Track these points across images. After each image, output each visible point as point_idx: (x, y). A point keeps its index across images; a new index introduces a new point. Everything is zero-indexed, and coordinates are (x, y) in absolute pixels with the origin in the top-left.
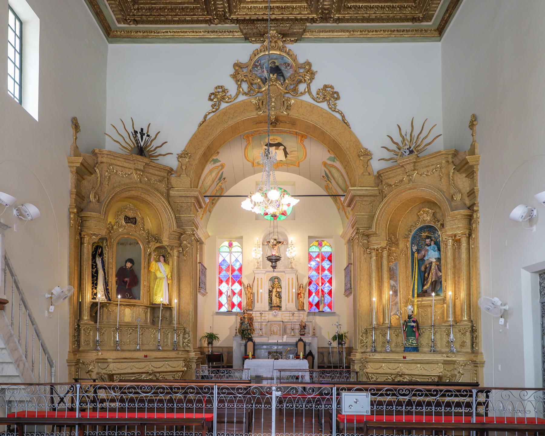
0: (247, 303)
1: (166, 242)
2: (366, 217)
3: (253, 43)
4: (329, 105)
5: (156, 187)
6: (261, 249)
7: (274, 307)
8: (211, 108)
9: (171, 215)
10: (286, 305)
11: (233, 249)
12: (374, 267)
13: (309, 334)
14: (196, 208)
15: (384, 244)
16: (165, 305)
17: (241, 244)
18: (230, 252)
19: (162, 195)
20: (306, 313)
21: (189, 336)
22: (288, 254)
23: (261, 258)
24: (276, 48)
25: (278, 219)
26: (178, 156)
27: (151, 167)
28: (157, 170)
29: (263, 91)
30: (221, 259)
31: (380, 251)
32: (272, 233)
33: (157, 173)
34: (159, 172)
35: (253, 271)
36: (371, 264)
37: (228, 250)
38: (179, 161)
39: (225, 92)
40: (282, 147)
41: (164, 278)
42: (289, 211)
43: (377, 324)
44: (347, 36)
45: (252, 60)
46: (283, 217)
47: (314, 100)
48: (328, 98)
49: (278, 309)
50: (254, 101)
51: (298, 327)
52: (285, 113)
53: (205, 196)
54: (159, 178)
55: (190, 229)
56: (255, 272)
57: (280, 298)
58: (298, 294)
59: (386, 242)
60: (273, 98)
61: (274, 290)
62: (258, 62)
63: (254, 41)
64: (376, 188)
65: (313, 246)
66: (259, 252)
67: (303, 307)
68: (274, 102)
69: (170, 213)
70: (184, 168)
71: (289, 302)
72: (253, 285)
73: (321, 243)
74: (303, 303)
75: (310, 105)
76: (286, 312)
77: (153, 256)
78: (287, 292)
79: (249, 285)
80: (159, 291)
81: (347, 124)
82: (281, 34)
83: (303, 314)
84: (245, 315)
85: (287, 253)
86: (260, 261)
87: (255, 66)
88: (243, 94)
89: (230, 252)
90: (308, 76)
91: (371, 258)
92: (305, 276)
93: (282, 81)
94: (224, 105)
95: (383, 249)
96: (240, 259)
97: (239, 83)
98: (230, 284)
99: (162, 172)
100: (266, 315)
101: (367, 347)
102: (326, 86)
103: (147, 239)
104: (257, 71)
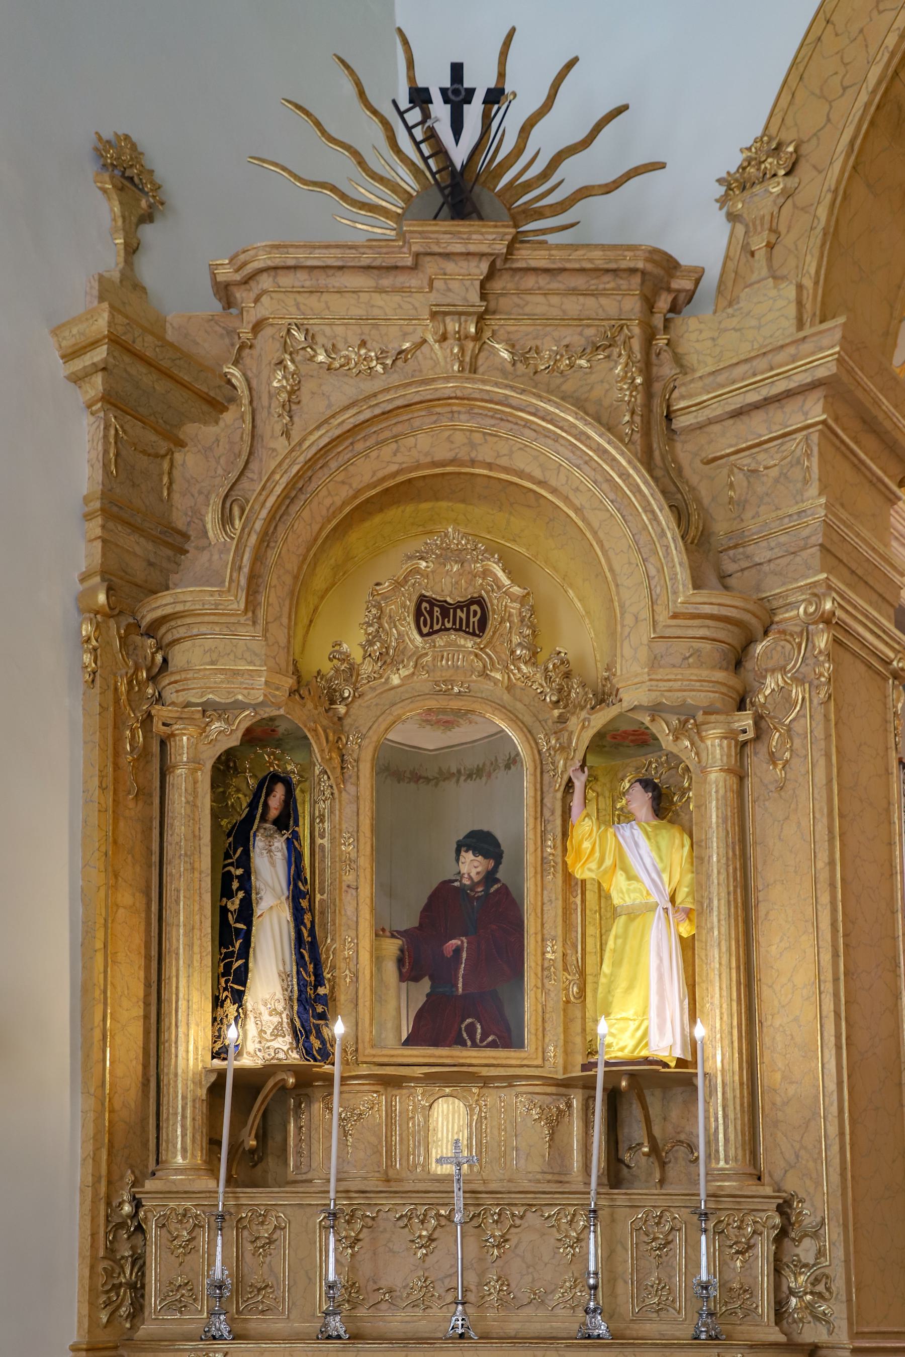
5: (568, 387)
19: (610, 428)
27: (530, 281)
28: (574, 292)
33: (573, 306)
34: (591, 302)
38: (732, 217)
41: (653, 908)
54: (590, 332)
70: (758, 243)
99: (603, 293)
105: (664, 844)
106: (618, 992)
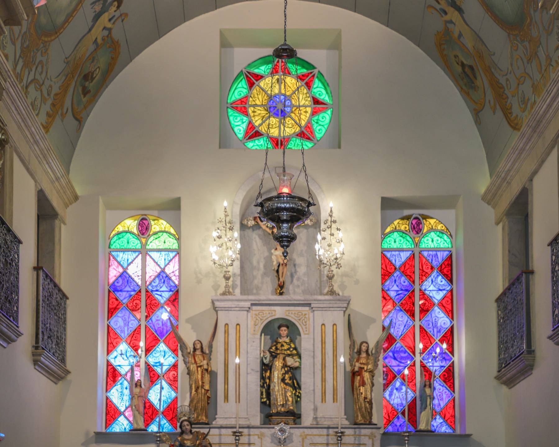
0: (191, 401)
6: (236, 234)
7: (278, 414)
10: (315, 410)
11: (153, 243)
17: (176, 224)
18: (144, 252)
20: (378, 434)
23: (237, 264)
30: (114, 272)
35: (213, 302)
37: (139, 246)
49: (291, 422)
56: (217, 304)
57: (295, 388)
58: (354, 374)
61: (278, 364)
65: (392, 232)
66: (229, 244)
67: (370, 414)
71: (323, 400)
72: (210, 346)
73: (419, 223)
74: (370, 403)
76: (315, 431)
78: (318, 366)
79: (198, 346)
83: (372, 436)
85: (317, 247)
86: (234, 275)
89: (144, 252)
92: (373, 321)
96: (172, 269)
98: (142, 344)
100: (254, 439)
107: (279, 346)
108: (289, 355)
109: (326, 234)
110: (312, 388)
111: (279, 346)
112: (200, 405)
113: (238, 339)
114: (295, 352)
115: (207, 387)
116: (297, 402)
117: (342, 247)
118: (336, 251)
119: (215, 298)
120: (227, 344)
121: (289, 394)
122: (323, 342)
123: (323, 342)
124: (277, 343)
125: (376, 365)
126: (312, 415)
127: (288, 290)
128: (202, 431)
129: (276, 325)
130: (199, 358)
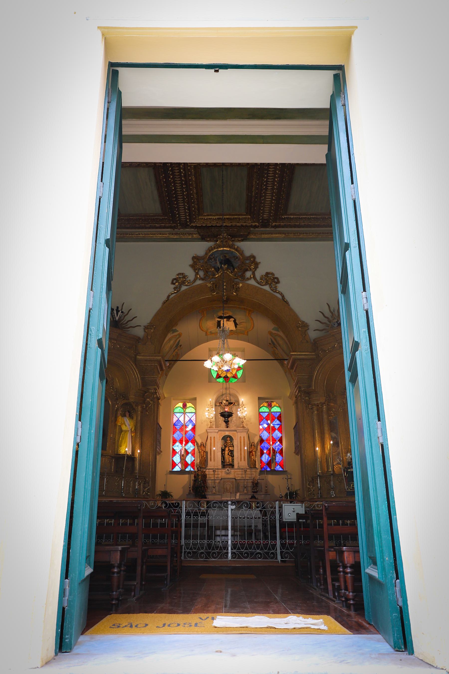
1: (132, 398)
2: (307, 377)
3: (208, 242)
4: (271, 288)
7: (227, 465)
8: (173, 290)
9: (138, 376)
10: (238, 463)
12: (315, 421)
13: (262, 491)
14: (158, 370)
15: (322, 400)
16: (128, 455)
21: (149, 485)
22: (239, 414)
24: (227, 245)
25: (230, 382)
26: (144, 328)
29: (217, 277)
31: (320, 406)
32: (224, 394)
36: (313, 418)
39: (185, 278)
40: (232, 320)
42: (240, 374)
43: (322, 473)
44: (283, 237)
45: (207, 254)
46: (235, 380)
47: (258, 284)
48: (270, 283)
50: (209, 285)
51: (250, 484)
52: (235, 294)
53: (166, 361)
55: (153, 388)
56: (208, 431)
57: (232, 457)
58: (250, 452)
59: (325, 398)
60: (225, 282)
61: (227, 449)
62: (212, 256)
63: (209, 240)
64: (314, 353)
67: (255, 465)
68: (225, 286)
69: (137, 374)
71: (241, 460)
72: (206, 444)
75: (255, 287)
76: (238, 470)
77: (119, 412)
78: (239, 450)
79: (202, 444)
80: (123, 442)
81: (287, 302)
82: (231, 236)
83: (256, 472)
84: (199, 472)
85: (238, 413)
86: (213, 421)
87: (210, 258)
88: (200, 280)
90: (253, 266)
91: (313, 413)
93: (232, 270)
94: (184, 288)
95: (322, 404)
97: (197, 271)
100: (219, 473)
101: (314, 495)
102: (267, 274)
103: (115, 397)
104: (211, 262)
105: (131, 421)
106: (123, 443)
107: (227, 443)
108: (230, 446)
109: (241, 409)
110: (237, 457)
111: (227, 443)
112: (203, 462)
113: (214, 441)
114: (232, 445)
115: (205, 457)
116: (233, 461)
117: (246, 413)
118: (244, 414)
119: (207, 429)
120: (211, 443)
121: (230, 459)
122: (241, 442)
123: (241, 442)
124: (227, 442)
125: (257, 449)
126: (237, 465)
127: (230, 425)
128: (204, 470)
129: (226, 437)
130: (202, 448)
